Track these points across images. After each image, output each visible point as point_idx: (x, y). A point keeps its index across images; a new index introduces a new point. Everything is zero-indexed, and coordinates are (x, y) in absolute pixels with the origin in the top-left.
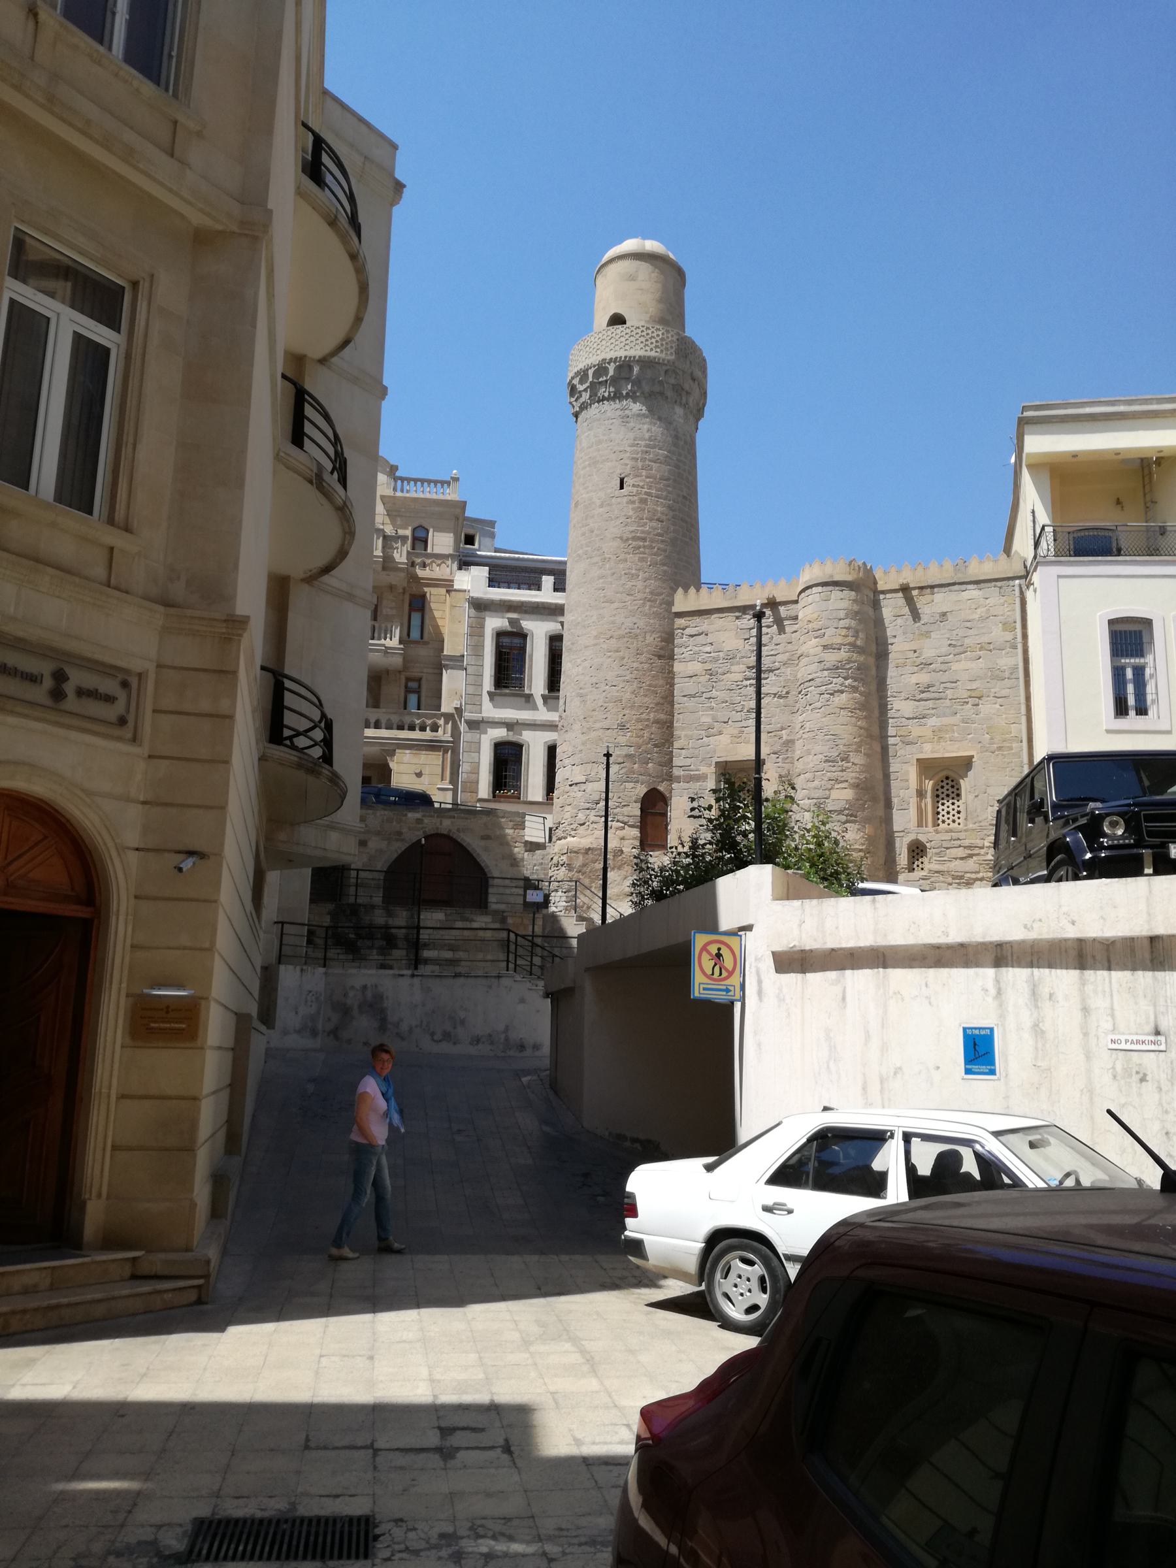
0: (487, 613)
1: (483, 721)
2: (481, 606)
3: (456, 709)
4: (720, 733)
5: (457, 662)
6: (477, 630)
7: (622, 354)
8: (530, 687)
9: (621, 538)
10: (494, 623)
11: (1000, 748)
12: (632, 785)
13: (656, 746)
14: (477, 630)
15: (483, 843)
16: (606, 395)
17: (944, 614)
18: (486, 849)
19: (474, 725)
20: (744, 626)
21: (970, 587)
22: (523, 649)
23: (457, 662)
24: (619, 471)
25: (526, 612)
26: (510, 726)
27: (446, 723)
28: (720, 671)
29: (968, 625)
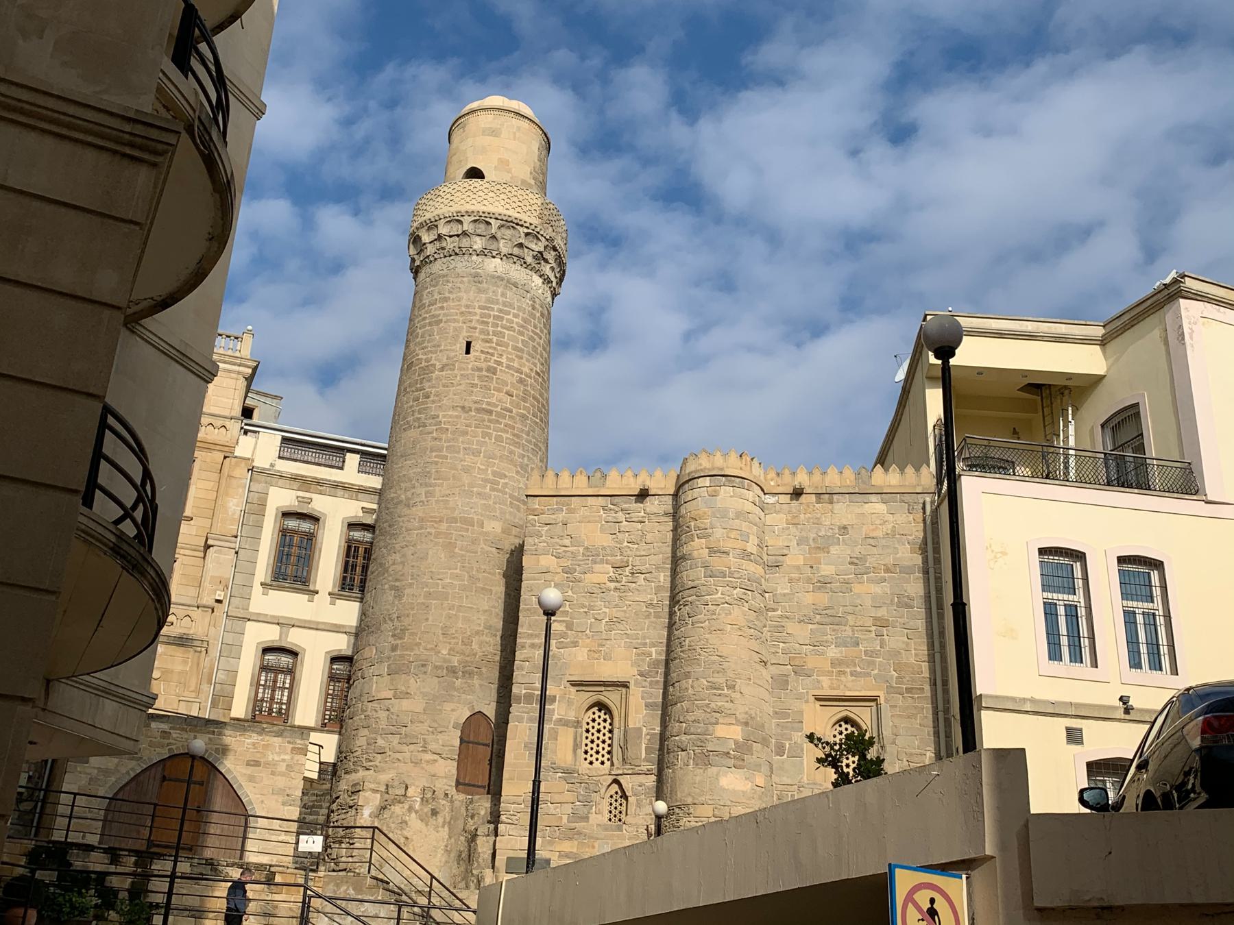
4: (575, 644)
9: (463, 408)
11: (909, 690)
15: (249, 770)
17: (845, 528)
18: (251, 779)
20: (610, 519)
21: (873, 498)
24: (465, 334)
29: (871, 541)
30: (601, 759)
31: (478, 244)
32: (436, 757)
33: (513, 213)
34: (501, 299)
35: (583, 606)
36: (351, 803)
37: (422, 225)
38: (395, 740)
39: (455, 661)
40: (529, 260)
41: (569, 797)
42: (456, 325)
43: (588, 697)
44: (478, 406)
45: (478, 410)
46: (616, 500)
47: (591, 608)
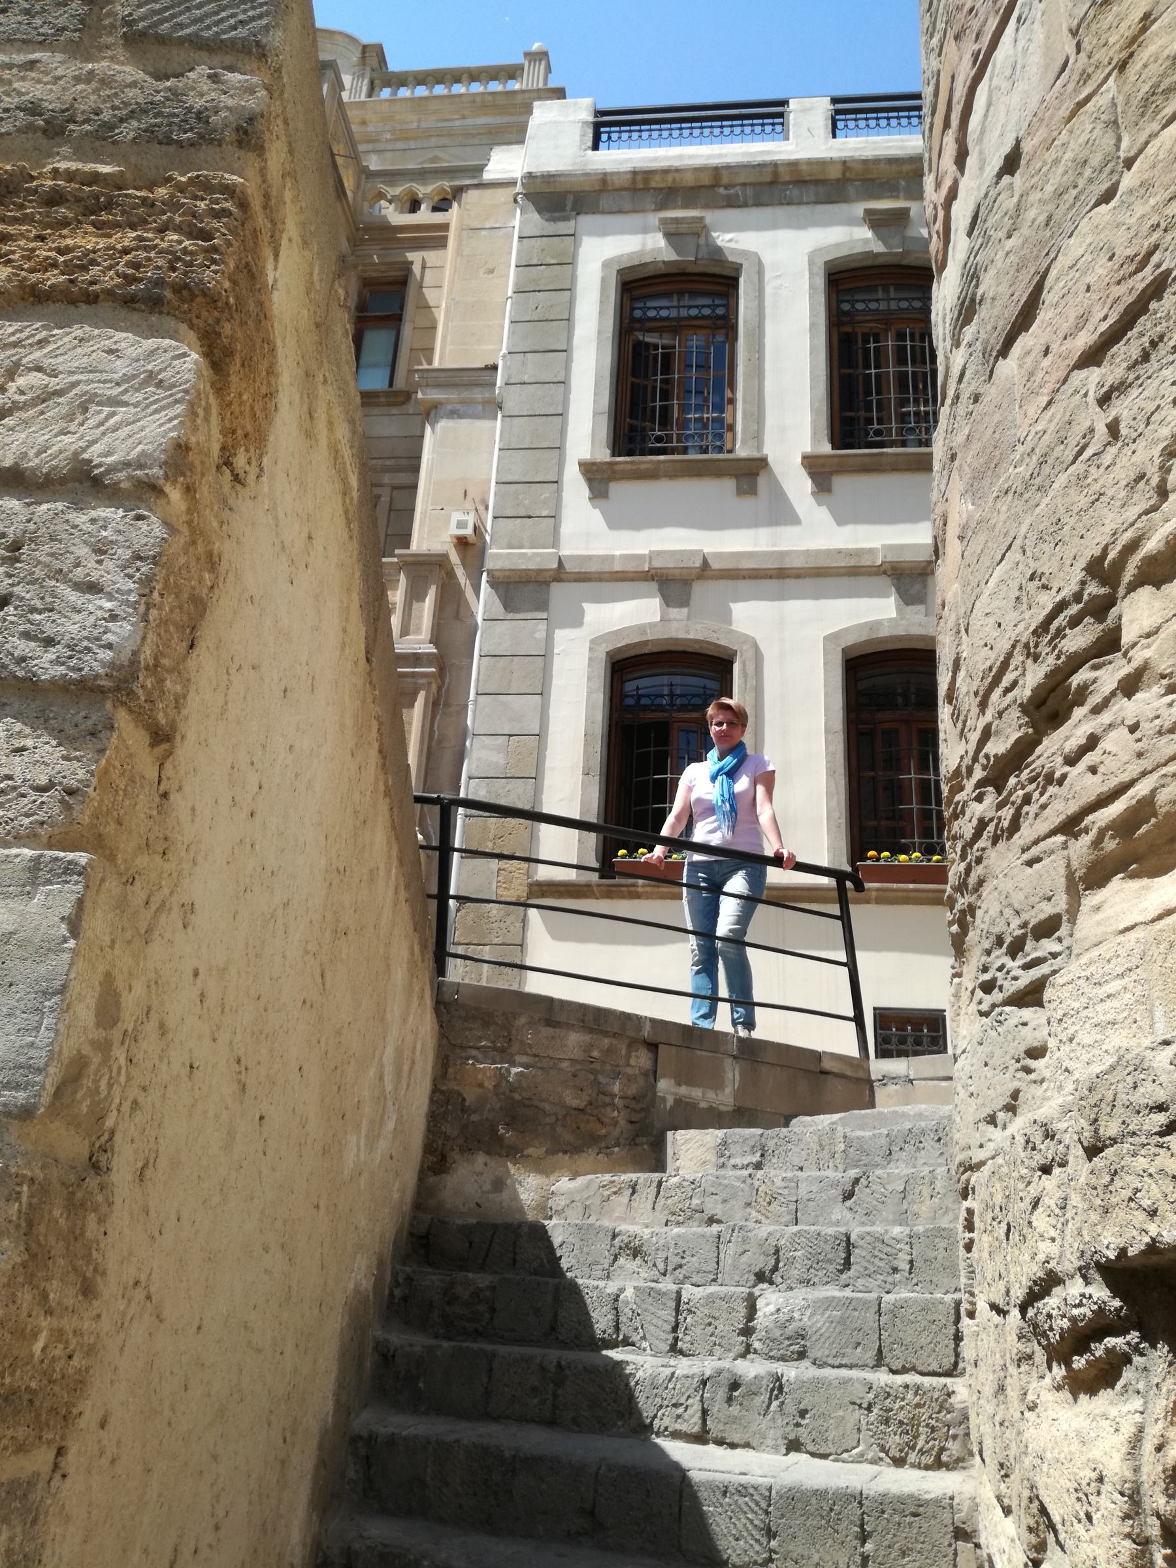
0: (585, 220)
1: (560, 574)
2: (559, 201)
3: (462, 543)
5: (474, 387)
6: (548, 279)
8: (758, 437)
10: (607, 249)
14: (548, 279)
19: (527, 591)
22: (726, 325)
23: (474, 387)
25: (731, 203)
26: (673, 582)
27: (415, 595)
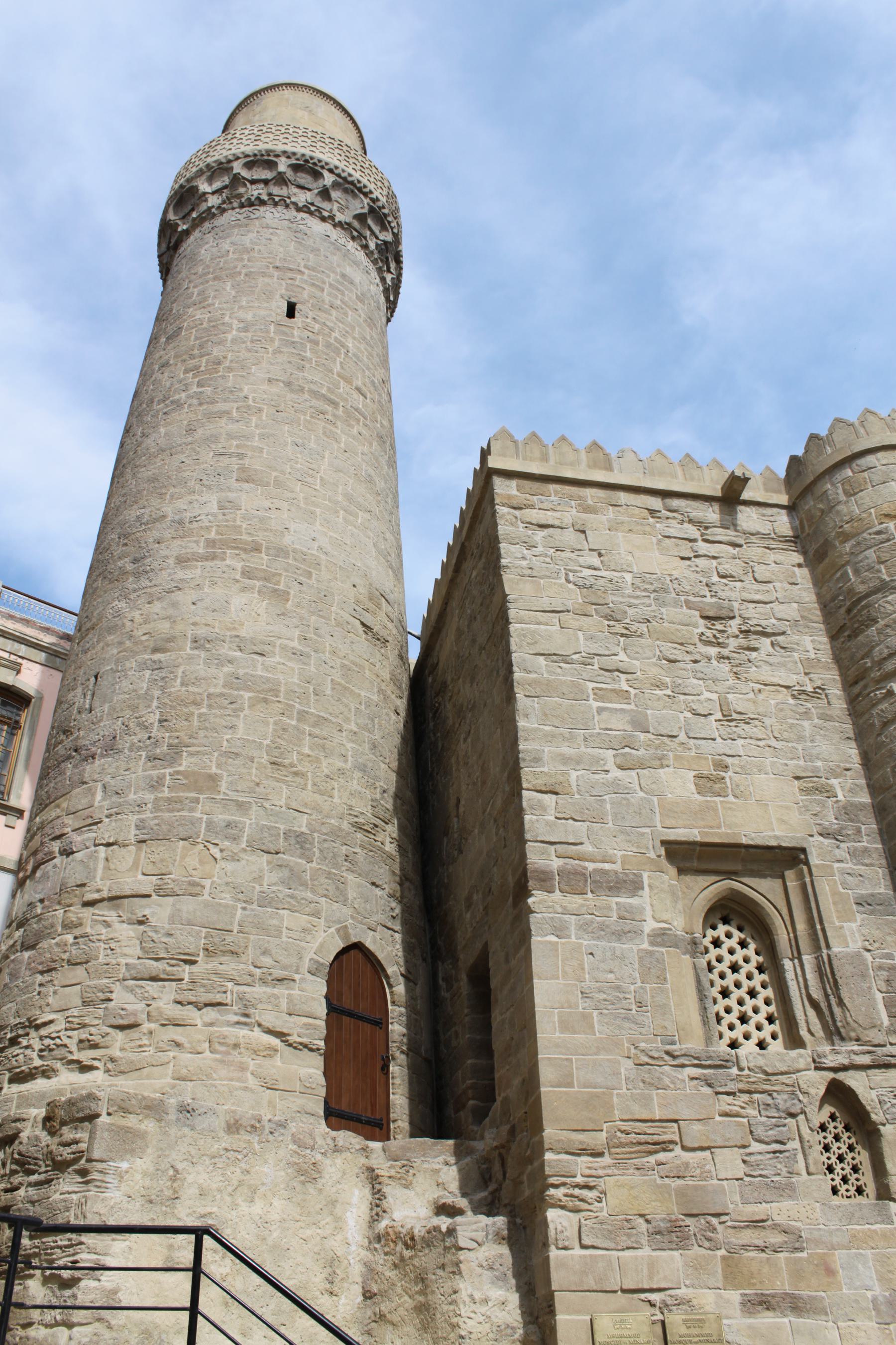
7: (307, 152)
9: (288, 384)
12: (304, 920)
13: (358, 827)
16: (265, 197)
28: (631, 611)
30: (756, 1036)
31: (302, 198)
32: (276, 1042)
33: (357, 175)
34: (338, 270)
35: (660, 685)
36: (66, 1153)
37: (200, 173)
38: (164, 998)
39: (302, 824)
40: (372, 246)
41: (733, 1130)
42: (267, 280)
43: (706, 889)
44: (314, 388)
45: (315, 394)
46: (675, 503)
47: (679, 690)
